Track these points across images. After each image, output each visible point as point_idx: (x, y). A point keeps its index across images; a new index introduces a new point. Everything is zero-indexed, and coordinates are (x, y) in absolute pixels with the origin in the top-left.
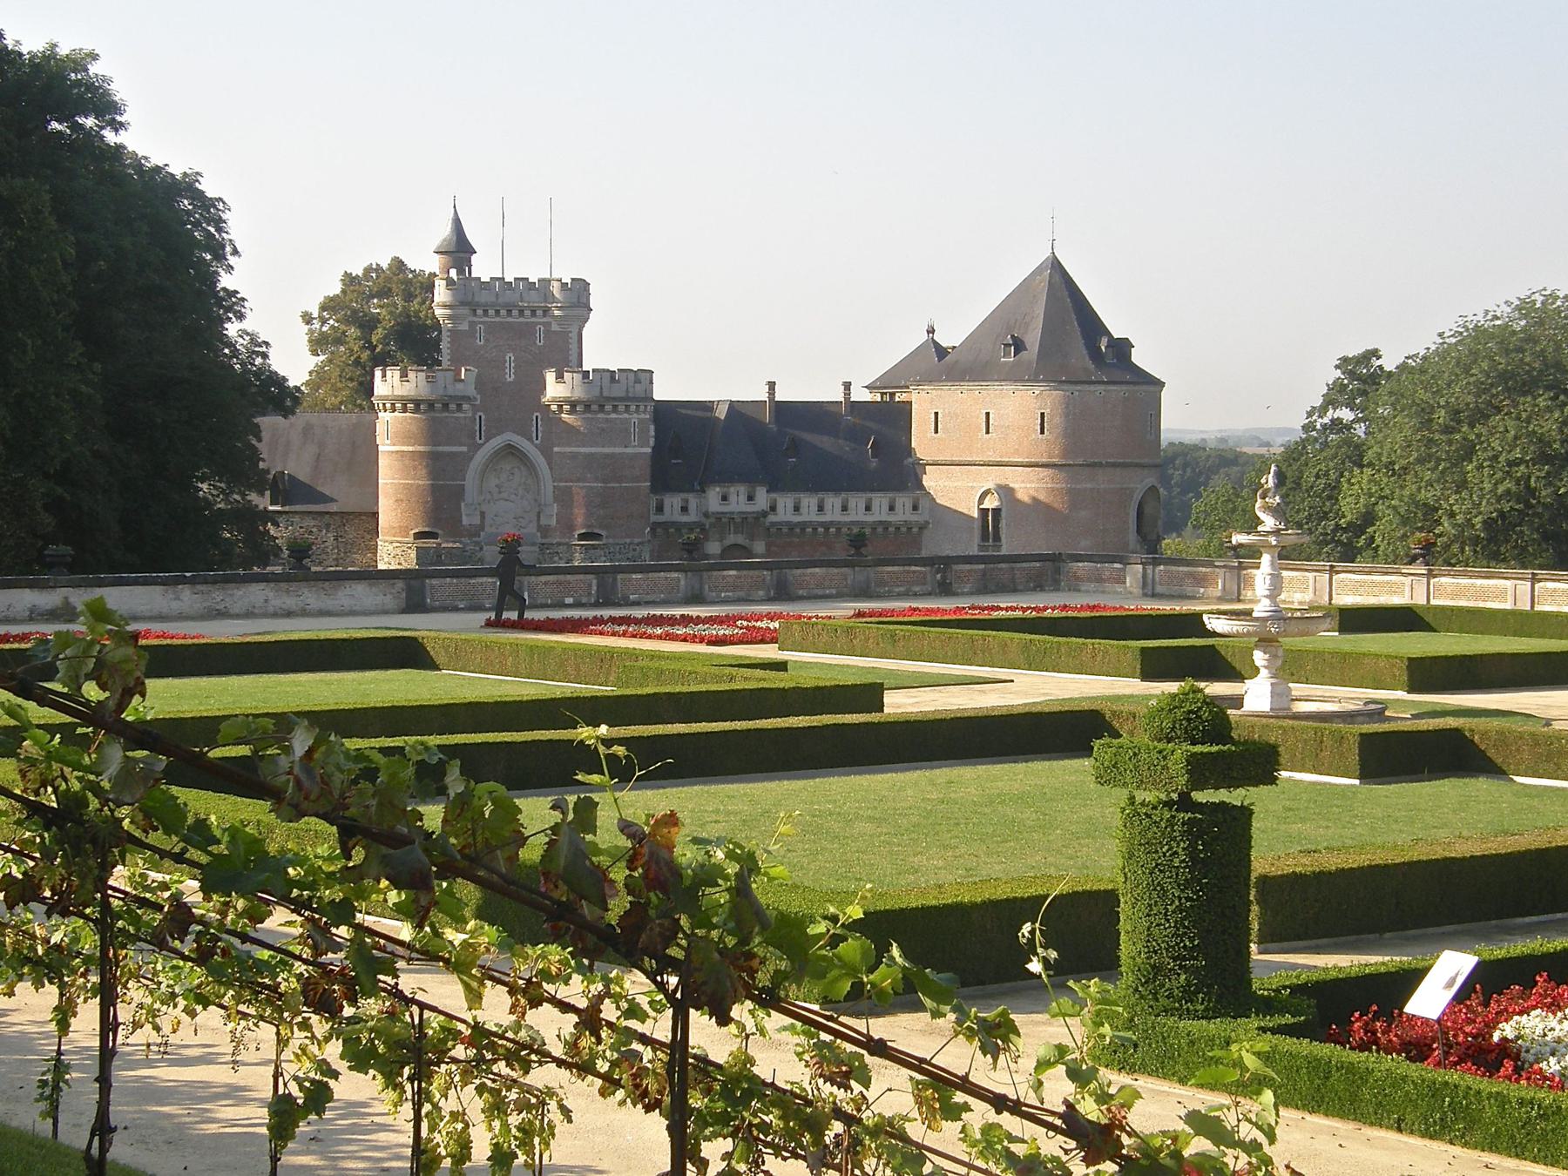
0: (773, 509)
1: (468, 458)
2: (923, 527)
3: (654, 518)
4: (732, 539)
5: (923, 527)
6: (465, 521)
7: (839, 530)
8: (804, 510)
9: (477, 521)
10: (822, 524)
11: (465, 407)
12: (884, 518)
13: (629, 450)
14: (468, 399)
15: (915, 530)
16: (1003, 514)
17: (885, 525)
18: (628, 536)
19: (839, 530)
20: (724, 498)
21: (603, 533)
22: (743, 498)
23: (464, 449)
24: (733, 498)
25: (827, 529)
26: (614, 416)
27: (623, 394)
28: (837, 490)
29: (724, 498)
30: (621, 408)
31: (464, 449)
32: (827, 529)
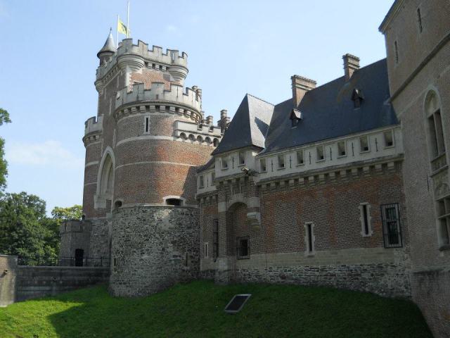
0: (264, 168)
1: (97, 166)
2: (398, 162)
3: (200, 192)
4: (237, 198)
5: (398, 162)
6: (96, 207)
7: (316, 177)
8: (287, 165)
9: (104, 206)
10: (301, 175)
11: (97, 137)
12: (358, 158)
13: (141, 138)
14: (97, 132)
15: (391, 165)
16: (441, 112)
17: (359, 166)
18: (137, 201)
19: (316, 177)
20: (225, 165)
21: (122, 200)
22: (237, 161)
23: (97, 162)
24: (230, 164)
25: (306, 178)
26: (131, 116)
27: (134, 100)
28: (310, 142)
29: (225, 165)
30: (134, 109)
31: (97, 162)
32: (306, 178)
